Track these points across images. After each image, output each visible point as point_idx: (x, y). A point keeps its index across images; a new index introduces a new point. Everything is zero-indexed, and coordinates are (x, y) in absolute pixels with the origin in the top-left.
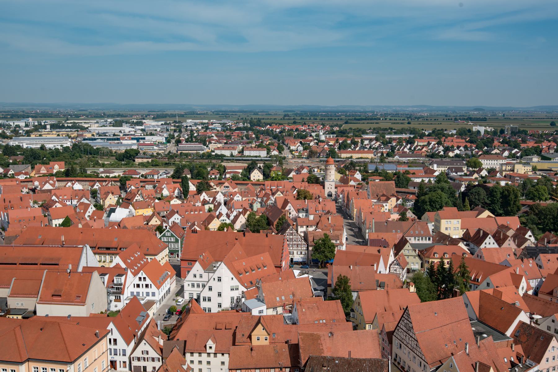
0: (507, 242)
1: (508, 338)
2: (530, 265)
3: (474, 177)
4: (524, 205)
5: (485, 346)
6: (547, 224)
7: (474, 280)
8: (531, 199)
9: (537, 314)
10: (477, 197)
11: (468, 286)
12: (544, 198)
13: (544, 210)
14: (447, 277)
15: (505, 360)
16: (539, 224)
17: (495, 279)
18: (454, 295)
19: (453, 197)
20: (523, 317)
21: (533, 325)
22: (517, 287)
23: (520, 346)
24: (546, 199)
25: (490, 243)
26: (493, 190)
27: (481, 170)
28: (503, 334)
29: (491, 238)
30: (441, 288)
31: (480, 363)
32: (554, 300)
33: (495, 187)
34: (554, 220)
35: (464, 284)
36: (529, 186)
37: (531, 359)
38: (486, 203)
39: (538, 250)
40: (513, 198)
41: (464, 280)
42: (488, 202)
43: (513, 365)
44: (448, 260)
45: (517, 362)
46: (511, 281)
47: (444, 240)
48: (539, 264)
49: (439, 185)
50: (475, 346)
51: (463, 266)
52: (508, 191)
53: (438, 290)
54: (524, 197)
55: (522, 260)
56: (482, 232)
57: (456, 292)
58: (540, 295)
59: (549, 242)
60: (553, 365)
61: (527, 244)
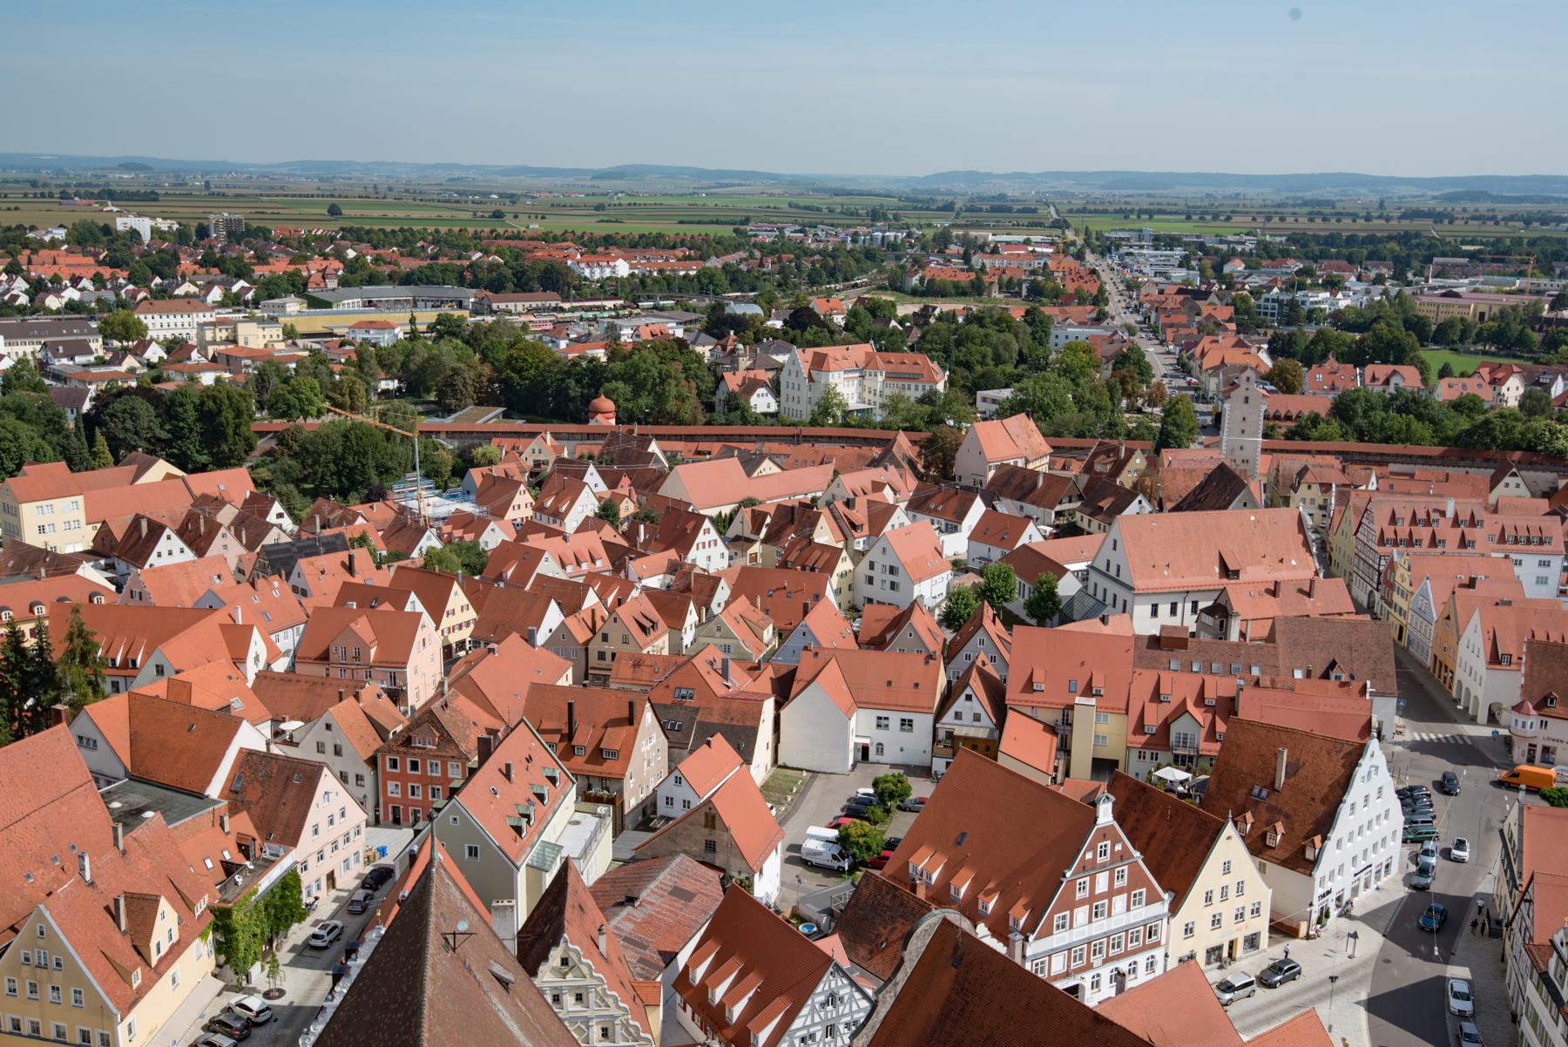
0: (218, 541)
1: (215, 802)
2: (276, 594)
3: (123, 368)
4: (262, 434)
5: (142, 845)
6: (323, 478)
7: (124, 665)
8: (283, 415)
9: (293, 718)
10: (129, 424)
11: (107, 687)
13: (312, 443)
14: (35, 674)
15: (209, 864)
16: (305, 479)
17: (174, 651)
18: (57, 718)
19: (58, 432)
20: (251, 737)
21: (275, 750)
22: (239, 660)
23: (244, 814)
24: (319, 414)
25: (170, 551)
27: (144, 345)
28: (200, 796)
29: (174, 537)
30: (21, 710)
31: (131, 898)
32: (335, 672)
33: (181, 392)
35: (90, 683)
36: (275, 380)
37: (276, 841)
38: (159, 439)
39: (295, 549)
40: (230, 415)
42: (164, 435)
43: (229, 869)
44: (32, 625)
45: (239, 859)
47: (32, 564)
50: (112, 854)
52: (214, 399)
53: (12, 719)
54: (265, 412)
55: (253, 584)
56: (144, 524)
57: (59, 712)
58: (300, 668)
59: (323, 527)
60: (332, 839)
61: (269, 540)
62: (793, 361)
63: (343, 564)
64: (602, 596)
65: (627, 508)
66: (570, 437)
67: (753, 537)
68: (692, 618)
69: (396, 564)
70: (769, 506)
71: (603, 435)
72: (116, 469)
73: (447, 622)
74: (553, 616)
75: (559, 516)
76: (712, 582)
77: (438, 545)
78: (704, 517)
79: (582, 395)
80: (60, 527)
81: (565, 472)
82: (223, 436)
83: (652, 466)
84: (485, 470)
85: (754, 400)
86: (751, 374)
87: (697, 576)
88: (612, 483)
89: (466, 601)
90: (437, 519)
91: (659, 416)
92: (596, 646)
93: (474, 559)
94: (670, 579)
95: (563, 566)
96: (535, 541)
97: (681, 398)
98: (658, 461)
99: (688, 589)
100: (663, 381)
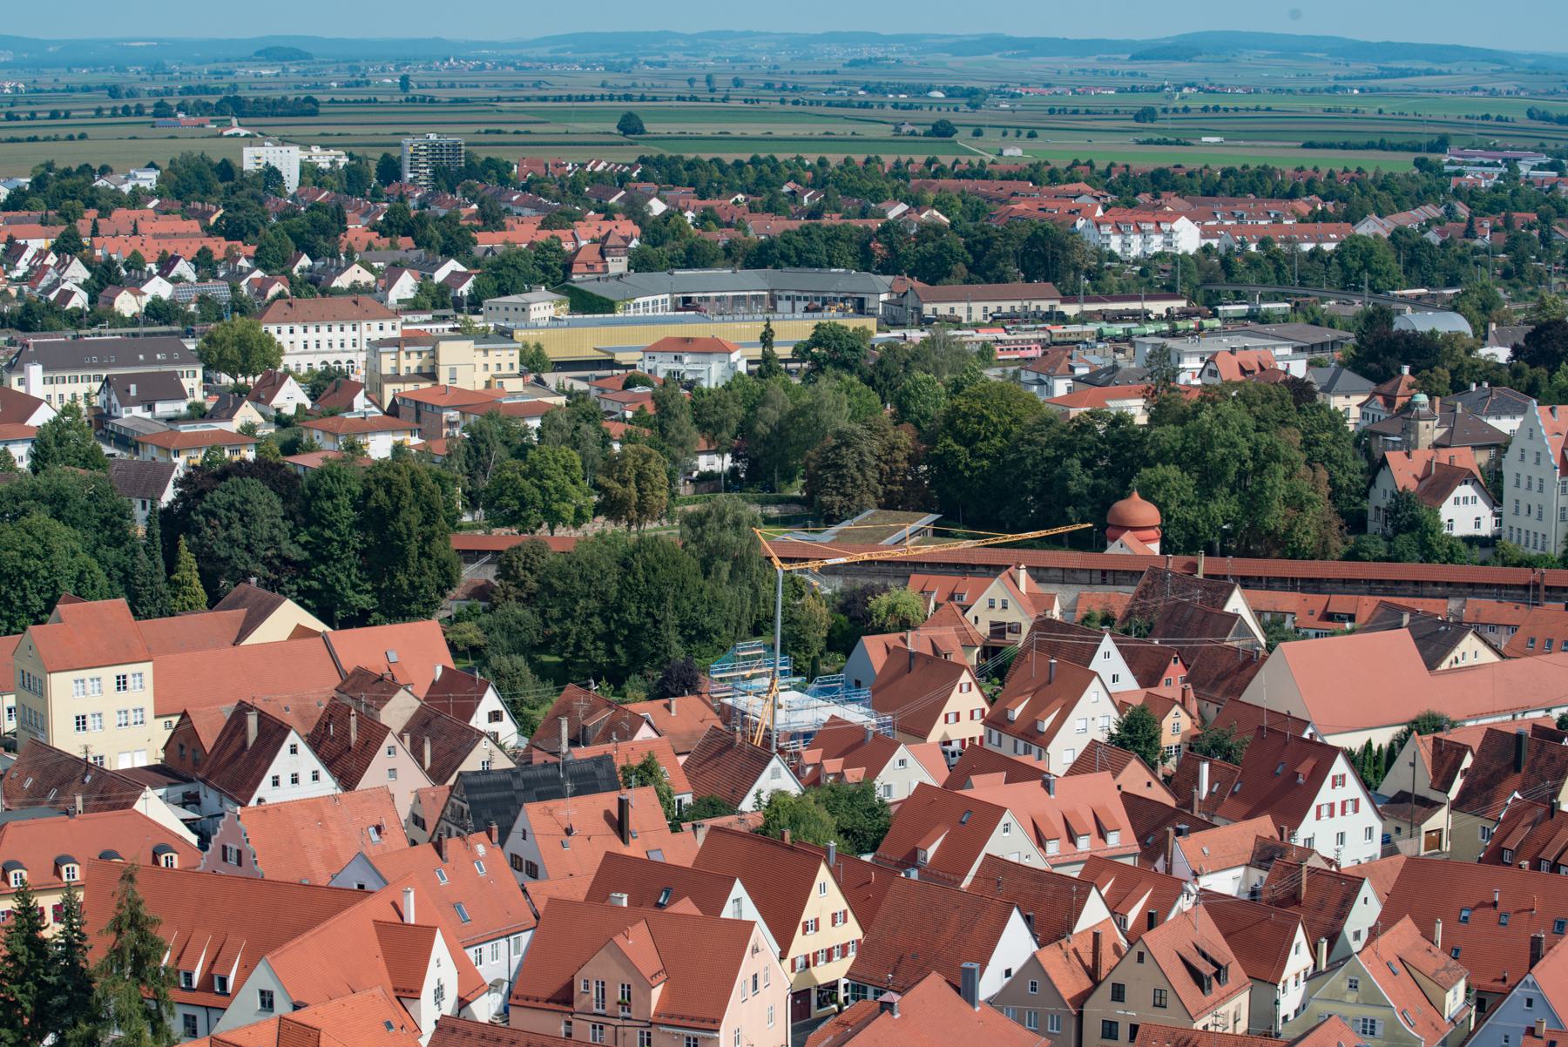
2: (481, 871)
3: (233, 426)
4: (471, 556)
6: (578, 646)
7: (207, 984)
8: (512, 519)
10: (237, 531)
11: (176, 1025)
12: (568, 510)
14: (59, 989)
16: (544, 648)
19: (118, 542)
22: (407, 992)
24: (580, 518)
25: (295, 776)
26: (314, 490)
27: (273, 383)
29: (303, 748)
34: (606, 621)
35: (147, 1014)
36: (499, 452)
38: (286, 561)
39: (518, 784)
40: (414, 517)
41: (145, 991)
42: (296, 553)
44: (56, 899)
46: (381, 962)
48: (526, 857)
49: (41, 478)
51: (132, 921)
52: (388, 486)
55: (438, 848)
56: (252, 720)
59: (574, 742)
61: (472, 763)
62: (1531, 432)
63: (608, 815)
64: (1116, 907)
65: (1175, 727)
66: (1067, 576)
67: (1435, 796)
68: (1299, 959)
69: (708, 823)
70: (1471, 732)
71: (1133, 576)
72: (211, 614)
73: (802, 944)
74: (1016, 943)
75: (1037, 739)
76: (1345, 886)
77: (792, 787)
78: (1334, 751)
79: (1094, 491)
80: (111, 719)
81: (1053, 650)
82: (400, 557)
83: (1232, 641)
84: (893, 638)
85: (1447, 510)
86: (1444, 456)
87: (1313, 871)
88: (1149, 676)
89: (841, 904)
90: (794, 736)
91: (1252, 539)
92: (1100, 1008)
93: (862, 821)
94: (1257, 876)
95: (1041, 842)
96: (986, 787)
97: (1297, 503)
98: (1245, 631)
99: (1294, 899)
100: (1260, 469)
